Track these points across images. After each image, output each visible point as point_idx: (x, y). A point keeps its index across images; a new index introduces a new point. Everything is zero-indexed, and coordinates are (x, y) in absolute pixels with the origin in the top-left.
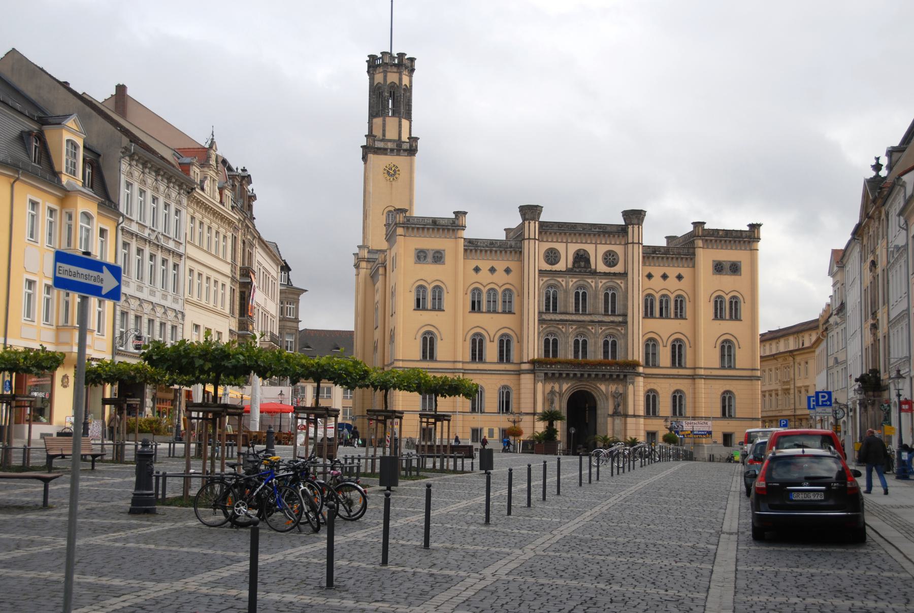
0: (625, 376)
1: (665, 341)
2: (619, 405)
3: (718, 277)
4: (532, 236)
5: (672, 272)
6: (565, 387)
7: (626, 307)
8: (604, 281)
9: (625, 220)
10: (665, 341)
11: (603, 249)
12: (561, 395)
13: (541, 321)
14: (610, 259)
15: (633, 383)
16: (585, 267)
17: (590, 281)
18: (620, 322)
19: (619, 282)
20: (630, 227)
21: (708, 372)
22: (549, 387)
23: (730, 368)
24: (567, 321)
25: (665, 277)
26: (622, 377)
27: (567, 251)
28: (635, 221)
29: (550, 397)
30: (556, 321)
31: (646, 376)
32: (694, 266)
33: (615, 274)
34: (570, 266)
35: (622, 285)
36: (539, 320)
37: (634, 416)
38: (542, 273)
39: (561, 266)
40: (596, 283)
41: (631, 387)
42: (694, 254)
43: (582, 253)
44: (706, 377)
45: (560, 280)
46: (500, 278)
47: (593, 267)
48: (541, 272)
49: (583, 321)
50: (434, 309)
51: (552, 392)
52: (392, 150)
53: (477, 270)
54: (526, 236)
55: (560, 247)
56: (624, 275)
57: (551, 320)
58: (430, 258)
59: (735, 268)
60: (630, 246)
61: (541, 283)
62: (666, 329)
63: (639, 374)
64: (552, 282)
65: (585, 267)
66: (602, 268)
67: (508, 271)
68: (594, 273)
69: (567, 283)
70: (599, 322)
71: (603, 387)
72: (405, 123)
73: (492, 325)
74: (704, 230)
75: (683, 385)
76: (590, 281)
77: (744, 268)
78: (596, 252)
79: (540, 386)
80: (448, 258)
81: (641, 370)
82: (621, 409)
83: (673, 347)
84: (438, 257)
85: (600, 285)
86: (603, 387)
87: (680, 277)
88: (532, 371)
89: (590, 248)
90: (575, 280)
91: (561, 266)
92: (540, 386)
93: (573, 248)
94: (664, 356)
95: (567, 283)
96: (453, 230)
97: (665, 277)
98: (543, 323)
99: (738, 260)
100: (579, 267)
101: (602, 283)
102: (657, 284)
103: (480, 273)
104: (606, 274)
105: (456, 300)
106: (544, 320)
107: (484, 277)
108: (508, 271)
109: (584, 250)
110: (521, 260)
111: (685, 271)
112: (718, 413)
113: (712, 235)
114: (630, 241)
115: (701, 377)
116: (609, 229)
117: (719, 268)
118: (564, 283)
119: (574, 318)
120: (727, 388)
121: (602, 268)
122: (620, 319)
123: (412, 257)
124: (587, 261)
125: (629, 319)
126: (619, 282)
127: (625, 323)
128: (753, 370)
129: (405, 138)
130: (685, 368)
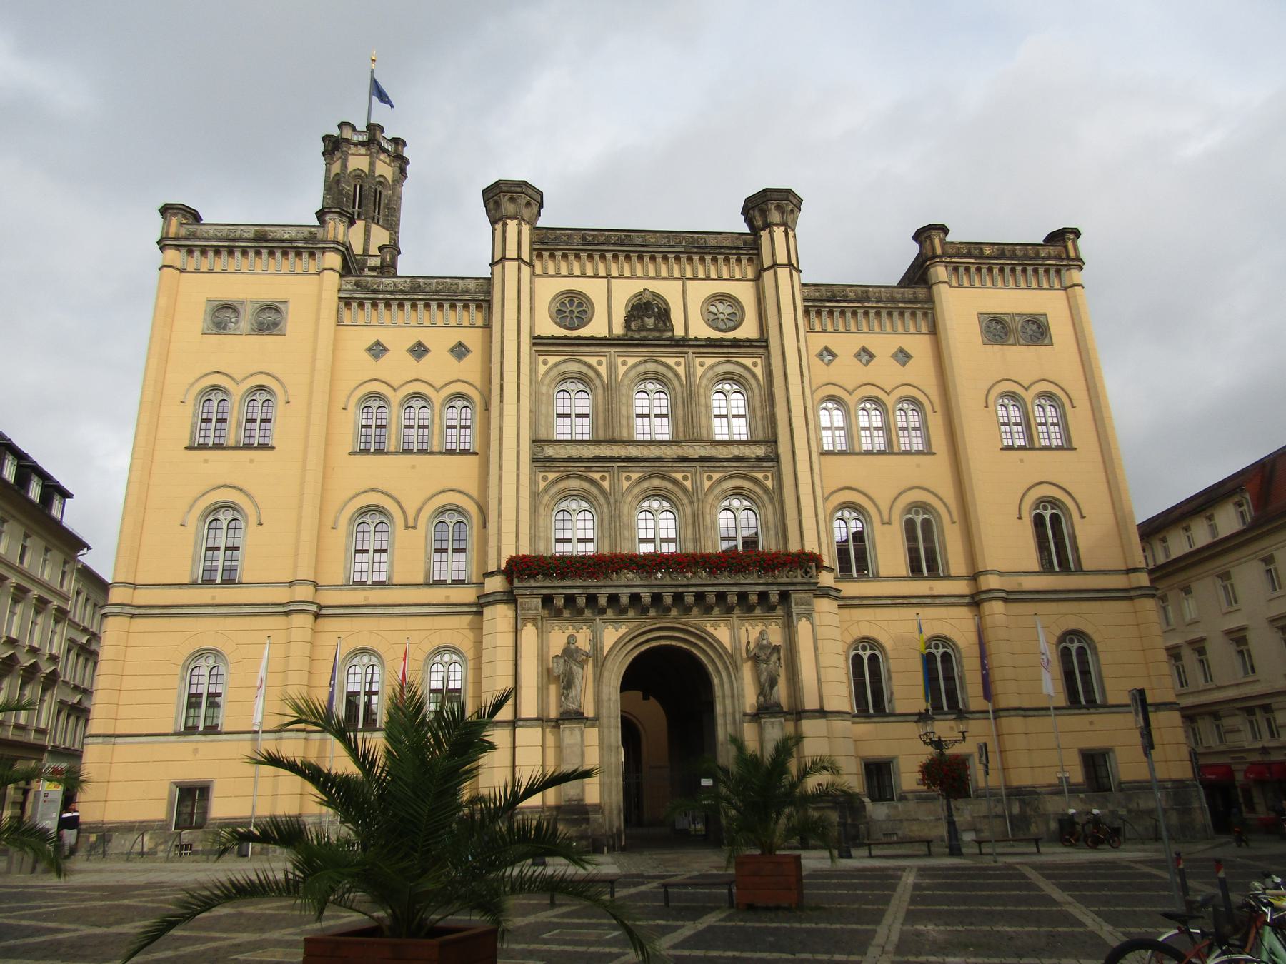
0: (785, 597)
1: (885, 508)
2: (773, 682)
5: (884, 343)
6: (611, 635)
8: (709, 362)
9: (749, 221)
10: (885, 508)
11: (700, 291)
12: (597, 657)
13: (541, 463)
15: (809, 615)
16: (656, 329)
17: (671, 361)
18: (758, 459)
19: (748, 362)
20: (765, 235)
22: (558, 638)
24: (612, 459)
25: (866, 355)
26: (774, 598)
27: (610, 295)
29: (560, 675)
30: (580, 459)
31: (847, 603)
32: (934, 331)
33: (735, 343)
34: (618, 330)
35: (758, 371)
36: (534, 460)
37: (822, 713)
40: (688, 366)
41: (803, 627)
42: (930, 299)
43: (647, 297)
45: (593, 361)
46: (440, 369)
47: (679, 332)
48: (538, 341)
49: (659, 459)
51: (569, 653)
55: (594, 289)
56: (760, 345)
57: (570, 459)
58: (246, 321)
59: (1036, 330)
60: (768, 276)
61: (542, 369)
63: (825, 592)
64: (574, 367)
65: (656, 329)
67: (460, 351)
69: (611, 368)
70: (702, 459)
71: (722, 633)
73: (413, 483)
74: (944, 243)
76: (671, 361)
77: (1060, 328)
78: (689, 298)
79: (529, 634)
80: (295, 320)
81: (826, 579)
82: (781, 692)
84: (269, 319)
85: (700, 371)
86: (722, 633)
87: (903, 356)
88: (510, 597)
89: (669, 290)
90: (631, 361)
92: (529, 633)
95: (611, 368)
96: (312, 255)
98: (550, 470)
99: (1042, 312)
100: (643, 328)
101: (704, 365)
103: (385, 359)
104: (710, 343)
106: (549, 459)
107: (398, 366)
108: (460, 351)
109: (655, 295)
113: (969, 255)
114: (767, 262)
115: (990, 594)
116: (712, 242)
117: (997, 329)
119: (634, 451)
121: (701, 330)
122: (760, 451)
124: (664, 315)
125: (783, 449)
126: (748, 362)
127: (775, 459)
128: (1128, 571)
130: (949, 577)
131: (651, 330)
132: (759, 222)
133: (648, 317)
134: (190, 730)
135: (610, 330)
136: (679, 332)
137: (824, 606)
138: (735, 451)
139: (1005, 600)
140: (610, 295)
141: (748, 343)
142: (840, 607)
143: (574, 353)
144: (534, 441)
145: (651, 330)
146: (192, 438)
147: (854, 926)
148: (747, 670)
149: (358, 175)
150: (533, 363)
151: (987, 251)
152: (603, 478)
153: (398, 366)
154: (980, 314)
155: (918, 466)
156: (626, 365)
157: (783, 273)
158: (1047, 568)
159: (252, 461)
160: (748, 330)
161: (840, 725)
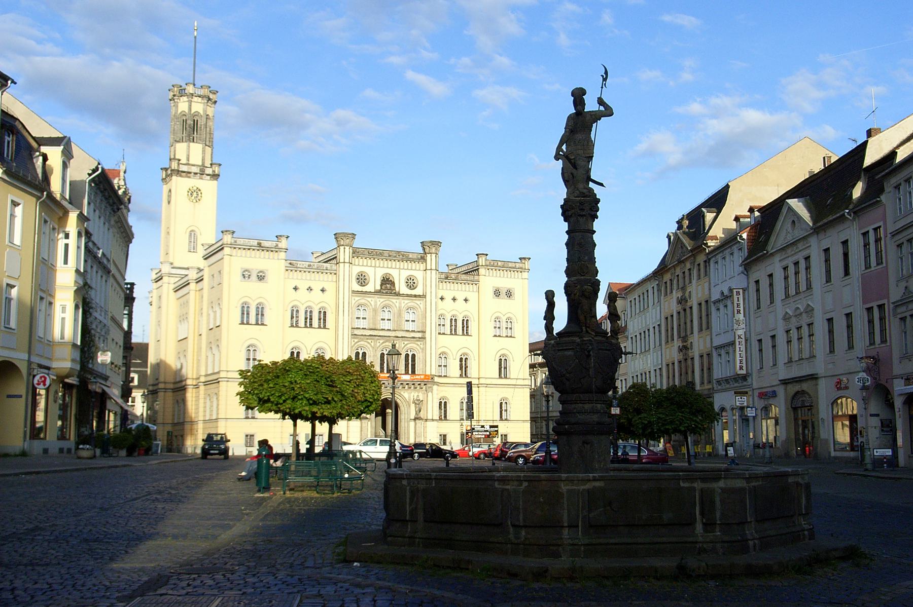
3: (497, 300)
4: (347, 260)
7: (424, 325)
8: (406, 302)
9: (424, 249)
11: (405, 274)
14: (411, 283)
17: (394, 301)
20: (429, 256)
21: (488, 381)
23: (506, 378)
28: (433, 250)
33: (415, 296)
34: (378, 288)
37: (433, 420)
39: (370, 288)
40: (400, 303)
41: (430, 394)
45: (369, 299)
47: (397, 289)
48: (353, 292)
50: (257, 324)
52: (196, 174)
53: (296, 289)
54: (342, 260)
55: (369, 271)
56: (424, 296)
58: (254, 277)
61: (353, 302)
62: (455, 345)
66: (404, 290)
68: (398, 294)
69: (376, 302)
71: (406, 395)
72: (208, 150)
80: (270, 277)
82: (422, 415)
83: (461, 359)
91: (370, 288)
94: (454, 369)
95: (376, 302)
97: (454, 299)
101: (405, 302)
102: (449, 309)
104: (408, 295)
105: (277, 316)
110: (337, 281)
114: (429, 268)
118: (373, 303)
121: (404, 290)
122: (420, 335)
124: (393, 284)
126: (418, 302)
129: (208, 164)
132: (427, 251)
133: (387, 283)
134: (247, 418)
137: (435, 387)
138: (413, 335)
141: (420, 296)
148: (413, 406)
149: (197, 114)
151: (500, 263)
153: (303, 293)
156: (380, 301)
157: (434, 272)
160: (418, 291)
161: (435, 423)
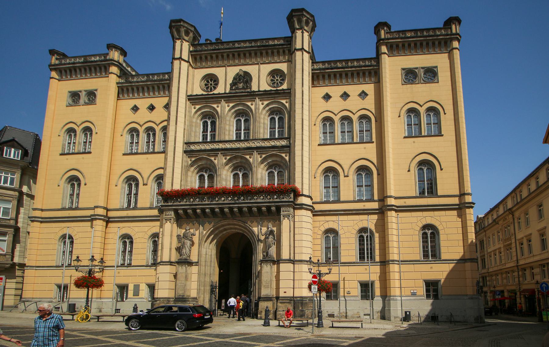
18: (283, 147)
24: (218, 150)
30: (205, 150)
35: (287, 105)
37: (293, 261)
38: (192, 99)
44: (399, 209)
45: (215, 106)
49: (238, 149)
65: (243, 88)
70: (257, 148)
75: (370, 222)
89: (252, 69)
93: (233, 71)
100: (237, 88)
106: (192, 151)
111: (369, 88)
112: (418, 254)
115: (392, 208)
120: (429, 221)
122: (284, 143)
123: (65, 98)
126: (284, 101)
131: (241, 89)
135: (225, 90)
136: (255, 88)
139: (396, 211)
140: (225, 75)
142: (314, 215)
143: (207, 102)
144: (186, 143)
145: (241, 89)
146: (63, 148)
147: (195, 344)
150: (190, 108)
152: (215, 159)
154: (403, 69)
155: (365, 148)
158: (422, 194)
159: (67, 159)
